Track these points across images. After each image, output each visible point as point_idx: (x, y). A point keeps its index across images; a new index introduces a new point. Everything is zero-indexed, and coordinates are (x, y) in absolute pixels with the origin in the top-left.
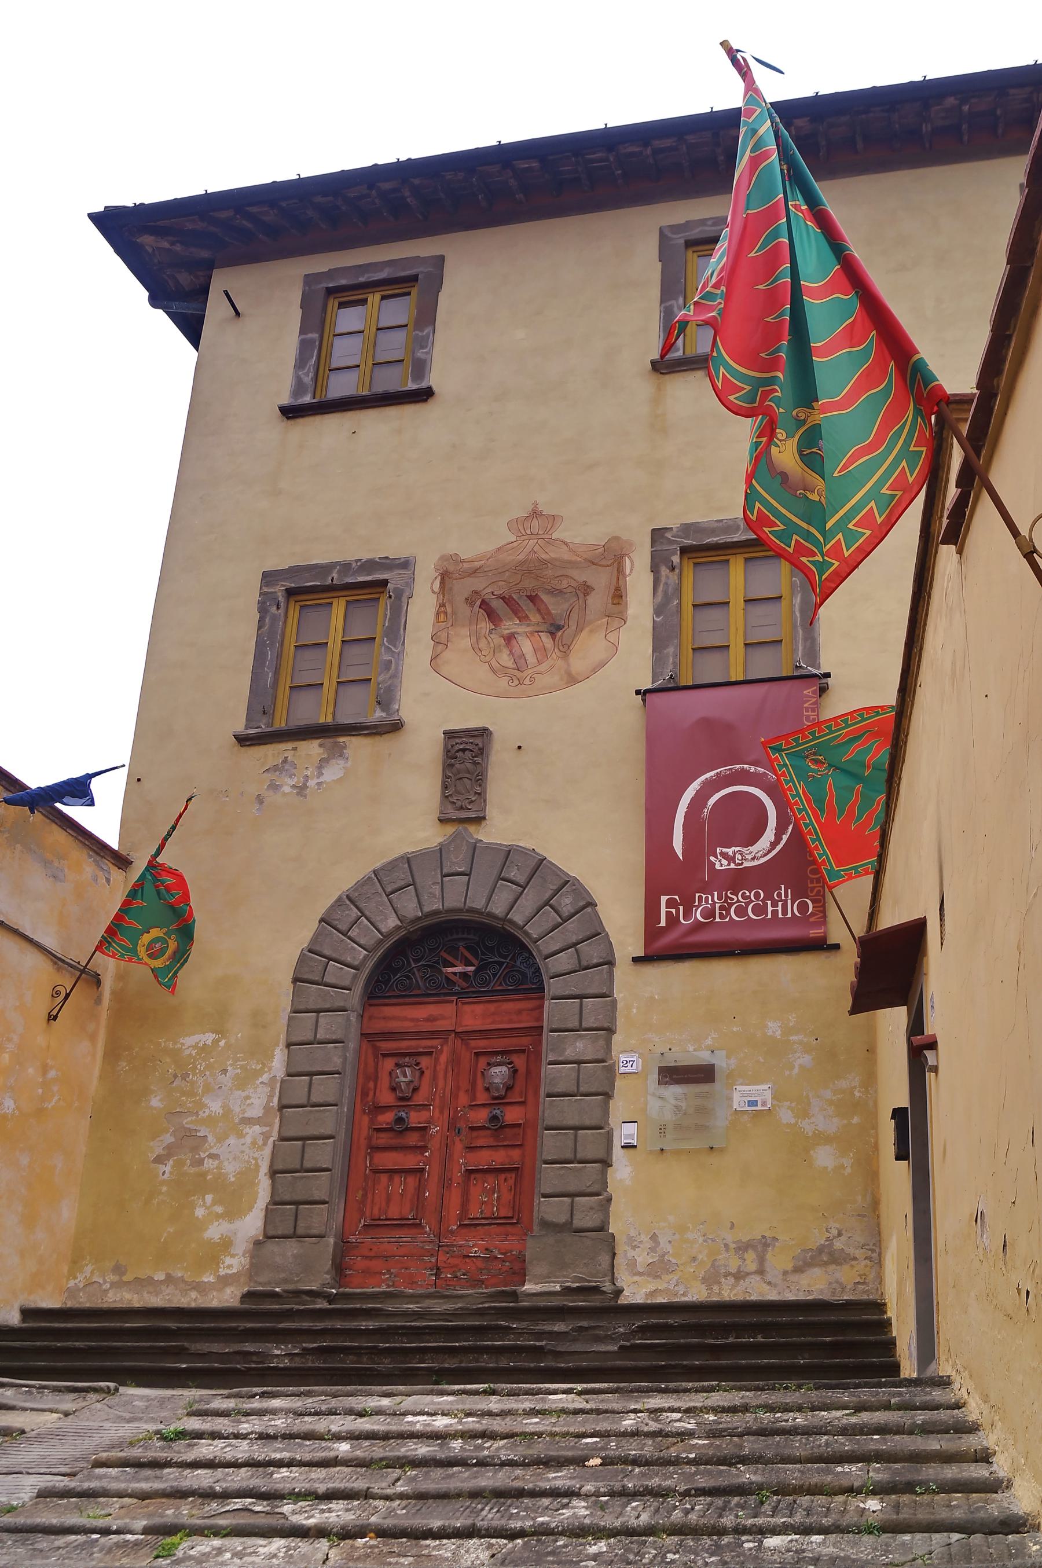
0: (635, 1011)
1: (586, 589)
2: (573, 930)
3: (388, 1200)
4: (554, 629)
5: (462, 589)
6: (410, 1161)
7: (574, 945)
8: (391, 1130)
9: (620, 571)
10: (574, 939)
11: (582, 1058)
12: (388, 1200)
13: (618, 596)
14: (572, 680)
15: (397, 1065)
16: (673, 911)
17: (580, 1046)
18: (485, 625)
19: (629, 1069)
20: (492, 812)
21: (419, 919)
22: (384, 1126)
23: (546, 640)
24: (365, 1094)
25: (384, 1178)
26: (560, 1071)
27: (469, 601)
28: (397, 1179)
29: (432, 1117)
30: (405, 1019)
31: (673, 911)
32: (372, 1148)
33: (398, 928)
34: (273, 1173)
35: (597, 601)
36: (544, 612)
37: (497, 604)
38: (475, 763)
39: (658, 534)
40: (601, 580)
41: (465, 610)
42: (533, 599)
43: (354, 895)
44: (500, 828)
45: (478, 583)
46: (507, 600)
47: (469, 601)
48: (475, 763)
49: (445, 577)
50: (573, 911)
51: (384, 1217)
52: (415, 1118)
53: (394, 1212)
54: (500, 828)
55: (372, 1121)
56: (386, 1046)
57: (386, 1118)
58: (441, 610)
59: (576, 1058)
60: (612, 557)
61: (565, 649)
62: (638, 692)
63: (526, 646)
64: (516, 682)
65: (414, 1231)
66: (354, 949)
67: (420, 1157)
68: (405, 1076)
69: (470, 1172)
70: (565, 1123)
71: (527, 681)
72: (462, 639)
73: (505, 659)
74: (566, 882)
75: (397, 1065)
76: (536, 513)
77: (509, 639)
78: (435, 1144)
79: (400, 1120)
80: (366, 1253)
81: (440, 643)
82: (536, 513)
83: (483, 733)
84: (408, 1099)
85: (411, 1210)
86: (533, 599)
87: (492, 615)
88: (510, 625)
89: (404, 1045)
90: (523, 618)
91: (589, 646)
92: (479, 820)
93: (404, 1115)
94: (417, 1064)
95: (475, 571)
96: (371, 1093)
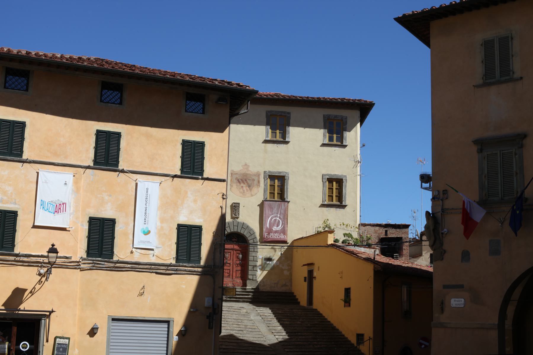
1: (254, 180)
2: (253, 237)
4: (249, 186)
5: (235, 176)
9: (259, 177)
13: (259, 182)
14: (252, 196)
17: (254, 254)
18: (238, 184)
20: (240, 216)
23: (248, 189)
27: (236, 179)
35: (256, 182)
36: (248, 183)
37: (240, 180)
39: (265, 172)
40: (256, 178)
41: (235, 181)
42: (246, 180)
44: (241, 219)
45: (237, 176)
46: (242, 180)
47: (236, 179)
49: (232, 174)
54: (241, 219)
58: (231, 181)
60: (258, 175)
61: (251, 190)
63: (245, 188)
72: (235, 186)
73: (241, 190)
74: (251, 229)
76: (246, 165)
77: (242, 187)
81: (231, 186)
82: (246, 165)
83: (239, 204)
86: (246, 180)
87: (239, 182)
88: (242, 185)
90: (244, 184)
91: (255, 190)
92: (237, 218)
95: (236, 174)
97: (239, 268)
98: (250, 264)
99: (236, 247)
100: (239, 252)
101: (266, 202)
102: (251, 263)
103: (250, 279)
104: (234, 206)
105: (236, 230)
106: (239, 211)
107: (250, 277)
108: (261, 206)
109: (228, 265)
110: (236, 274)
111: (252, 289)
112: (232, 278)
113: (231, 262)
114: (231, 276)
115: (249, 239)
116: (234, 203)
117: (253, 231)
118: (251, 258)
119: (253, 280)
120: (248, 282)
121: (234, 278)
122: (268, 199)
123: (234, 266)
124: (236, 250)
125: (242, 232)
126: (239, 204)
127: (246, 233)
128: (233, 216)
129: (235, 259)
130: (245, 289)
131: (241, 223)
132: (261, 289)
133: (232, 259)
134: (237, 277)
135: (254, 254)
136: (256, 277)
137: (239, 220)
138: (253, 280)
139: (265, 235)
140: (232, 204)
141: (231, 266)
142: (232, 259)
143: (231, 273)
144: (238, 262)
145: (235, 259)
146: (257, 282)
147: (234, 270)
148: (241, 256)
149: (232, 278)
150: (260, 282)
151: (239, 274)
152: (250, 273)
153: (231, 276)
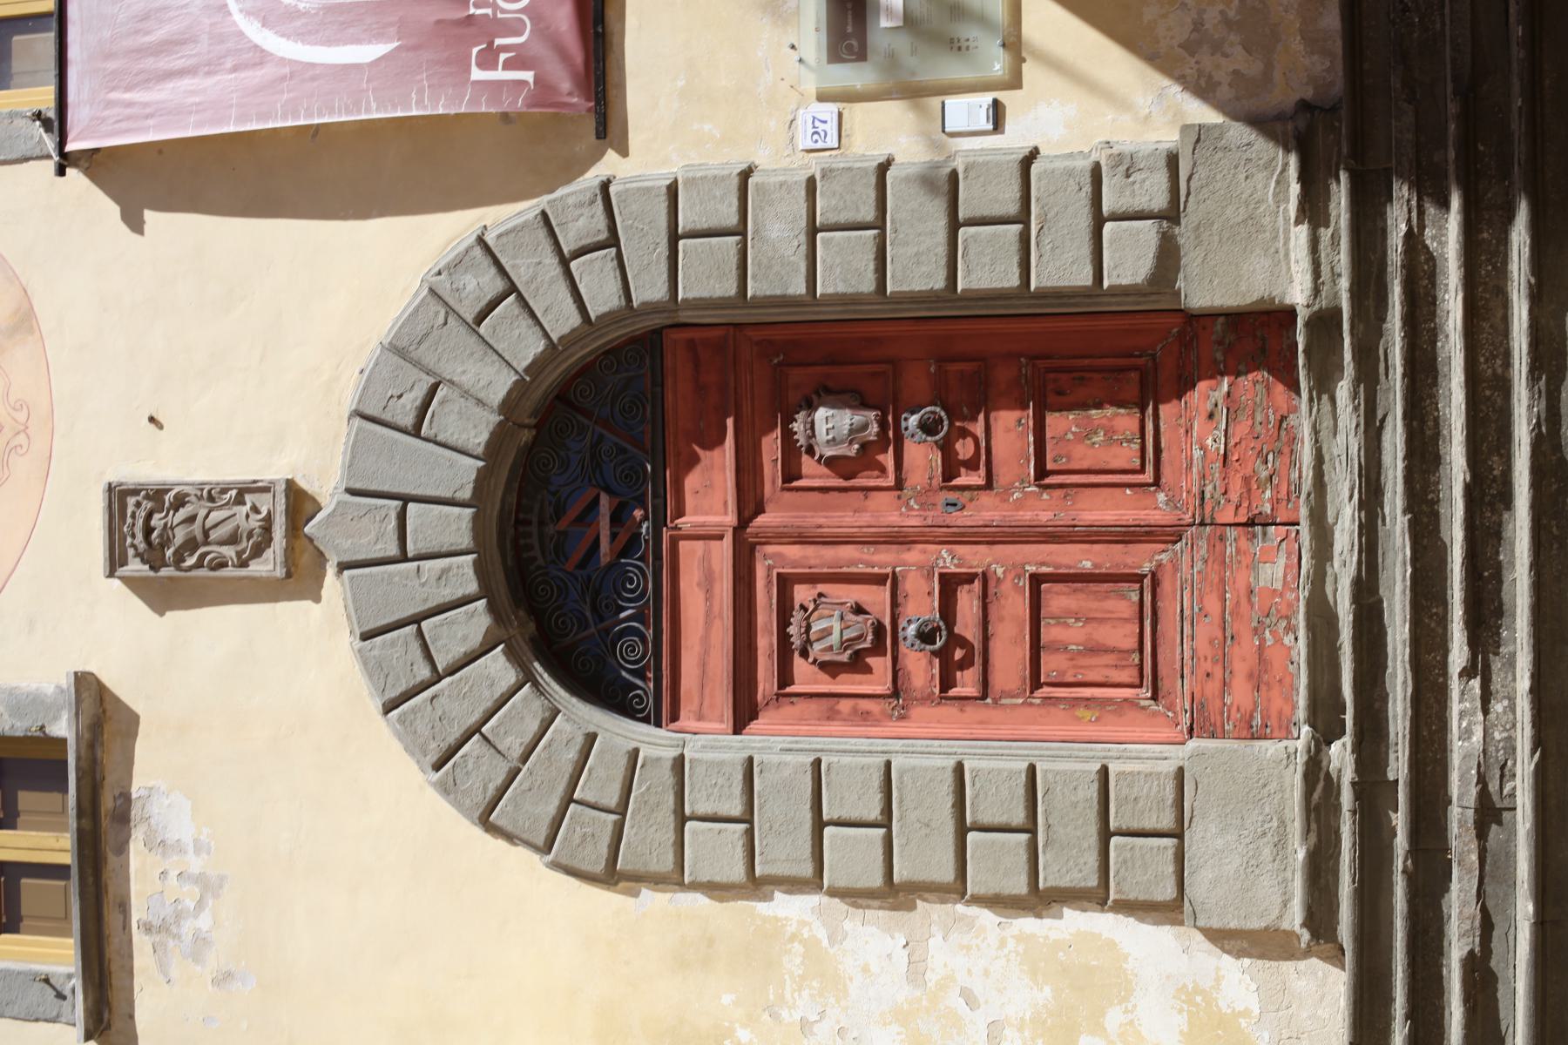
0: (707, 127)
3: (1094, 650)
6: (1013, 606)
7: (565, 262)
8: (944, 655)
10: (551, 261)
11: (803, 223)
12: (1094, 650)
15: (804, 654)
16: (503, 57)
19: (832, 128)
20: (275, 470)
21: (492, 608)
22: (936, 671)
24: (865, 717)
25: (1051, 665)
26: (829, 268)
28: (1049, 633)
29: (920, 567)
30: (706, 639)
31: (503, 57)
32: (984, 696)
33: (512, 655)
34: (1040, 899)
38: (180, 501)
43: (433, 757)
48: (180, 501)
50: (493, 270)
51: (1136, 658)
52: (921, 607)
53: (1124, 636)
55: (927, 699)
56: (766, 681)
57: (920, 667)
59: (803, 238)
62: (61, 171)
64: (22, 438)
65: (1166, 586)
66: (549, 745)
67: (1006, 587)
68: (827, 632)
69: (1041, 472)
70: (942, 251)
71: (22, 416)
75: (804, 654)
78: (975, 558)
79: (926, 636)
80: (1213, 687)
83: (117, 496)
84: (879, 629)
85: (1123, 597)
89: (766, 642)
93: (912, 630)
94: (804, 608)
96: (865, 704)
97: (1009, 430)
98: (928, 278)
99: (708, 494)
100: (771, 446)
101: (77, 116)
102: (916, 270)
103: (1168, 257)
104: (153, 555)
105: (456, 526)
106: (211, 494)
107: (1129, 259)
108: (144, 179)
109: (967, 603)
110: (1101, 478)
111: (1313, 210)
112: (1170, 535)
113: (918, 568)
114: (1142, 558)
115: (562, 320)
116: (115, 562)
117: (456, 265)
118: (844, 270)
119: (1171, 214)
120: (1208, 287)
121: (1157, 510)
122: (44, 98)
123: (986, 511)
124: (749, 502)
125: (476, 430)
126: (117, 496)
127: (485, 379)
128: (268, 566)
129: (885, 512)
130: (1325, 323)
131: (356, 451)
132: (1306, 64)
133: (882, 559)
134: (1151, 467)
135: (777, 231)
136: (1128, 165)
137: (326, 485)
138: (1171, 214)
139: (493, 82)
140: (132, 583)
141: (975, 558)
142: (882, 559)
143: (1084, 559)
144: (922, 457)
145: (885, 512)
146: (1199, 135)
147: (1044, 510)
148: (831, 424)
149: (1170, 535)
150: (1203, 89)
151: (1097, 435)
152: (1061, 266)
153: (1142, 558)
